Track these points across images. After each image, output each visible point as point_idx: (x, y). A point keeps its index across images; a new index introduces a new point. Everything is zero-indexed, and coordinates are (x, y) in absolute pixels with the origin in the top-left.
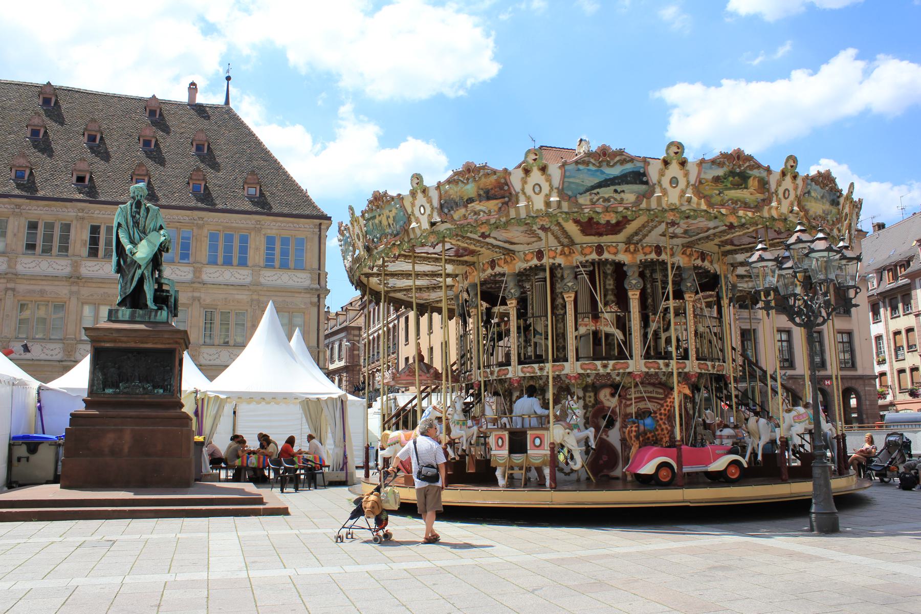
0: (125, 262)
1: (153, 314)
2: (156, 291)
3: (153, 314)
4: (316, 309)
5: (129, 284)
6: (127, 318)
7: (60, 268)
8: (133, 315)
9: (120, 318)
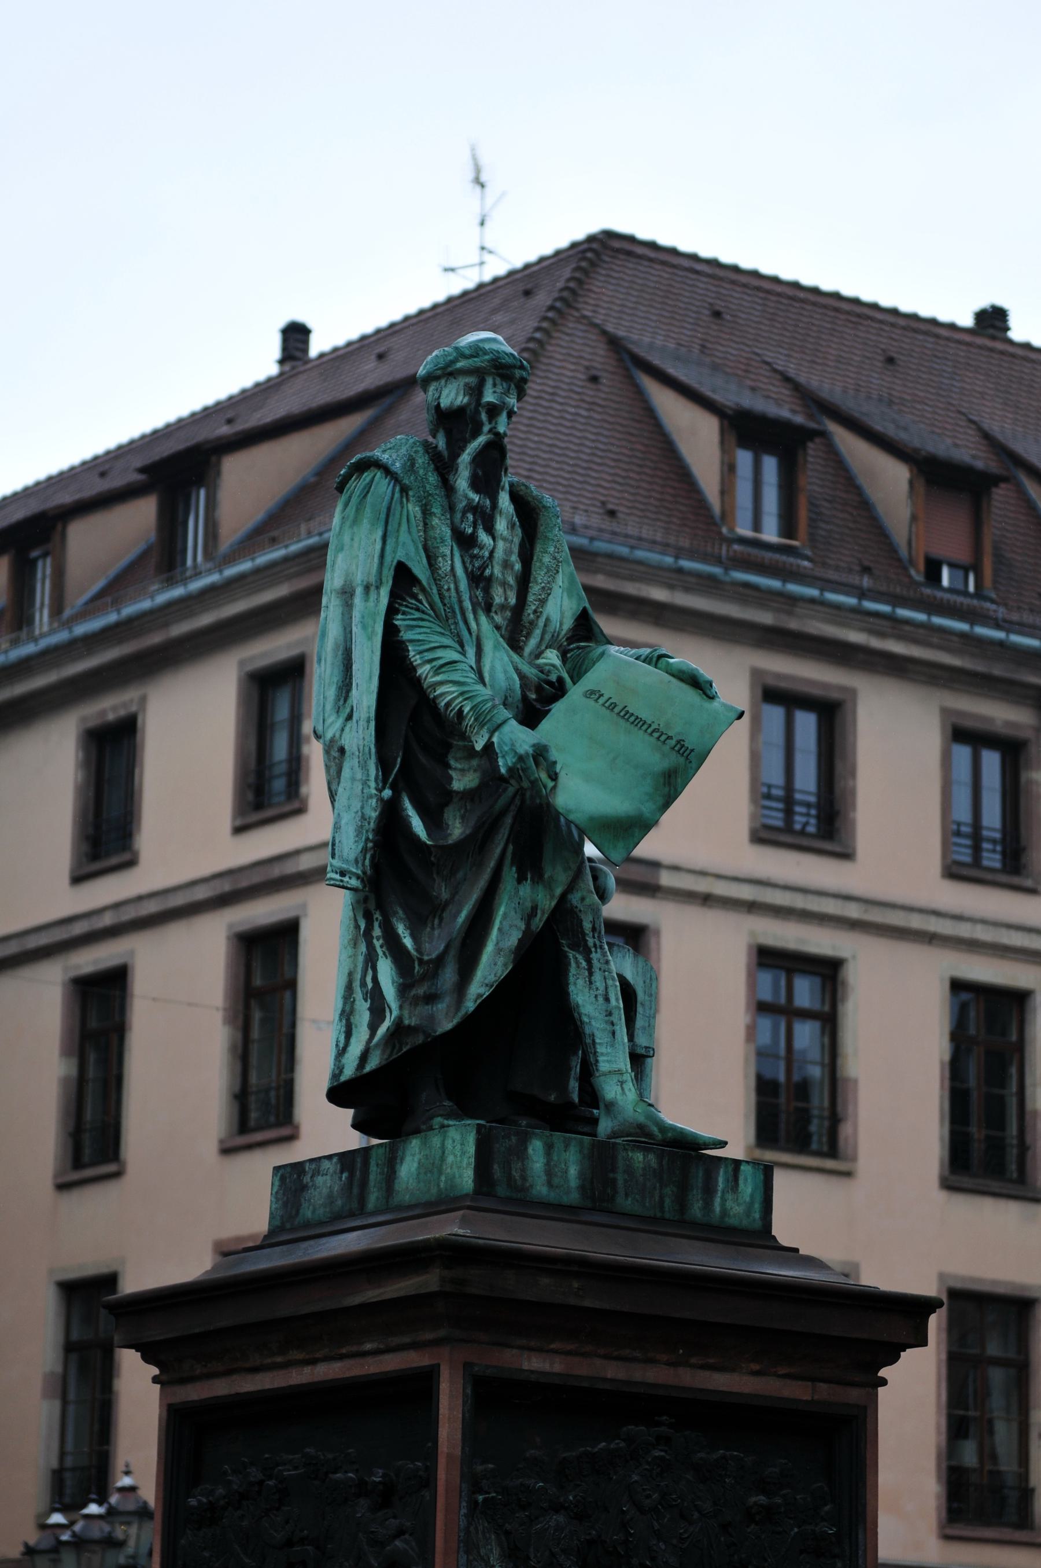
0: (433, 819)
5: (449, 975)
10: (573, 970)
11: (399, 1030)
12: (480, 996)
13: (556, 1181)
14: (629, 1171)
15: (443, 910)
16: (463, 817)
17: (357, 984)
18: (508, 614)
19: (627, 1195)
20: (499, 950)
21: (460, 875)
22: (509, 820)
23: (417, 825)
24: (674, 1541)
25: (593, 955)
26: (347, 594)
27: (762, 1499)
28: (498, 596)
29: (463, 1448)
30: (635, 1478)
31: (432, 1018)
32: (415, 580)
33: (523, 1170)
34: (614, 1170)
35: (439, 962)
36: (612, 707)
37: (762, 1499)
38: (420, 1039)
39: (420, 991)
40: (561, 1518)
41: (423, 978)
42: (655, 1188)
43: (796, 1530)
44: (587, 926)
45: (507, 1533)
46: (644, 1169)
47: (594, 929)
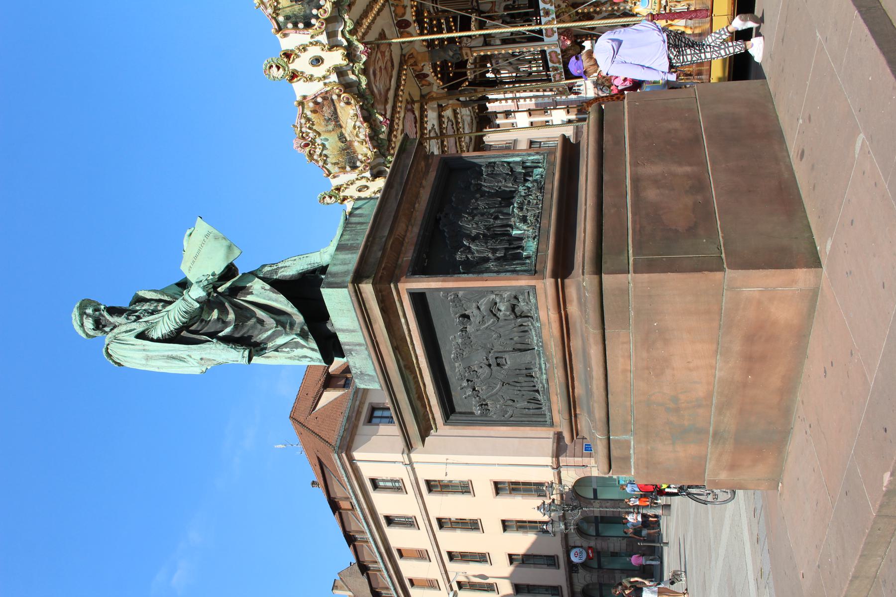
10: (284, 273)
11: (303, 335)
17: (289, 355)
20: (276, 301)
26: (148, 358)
28: (160, 308)
36: (194, 262)
38: (306, 328)
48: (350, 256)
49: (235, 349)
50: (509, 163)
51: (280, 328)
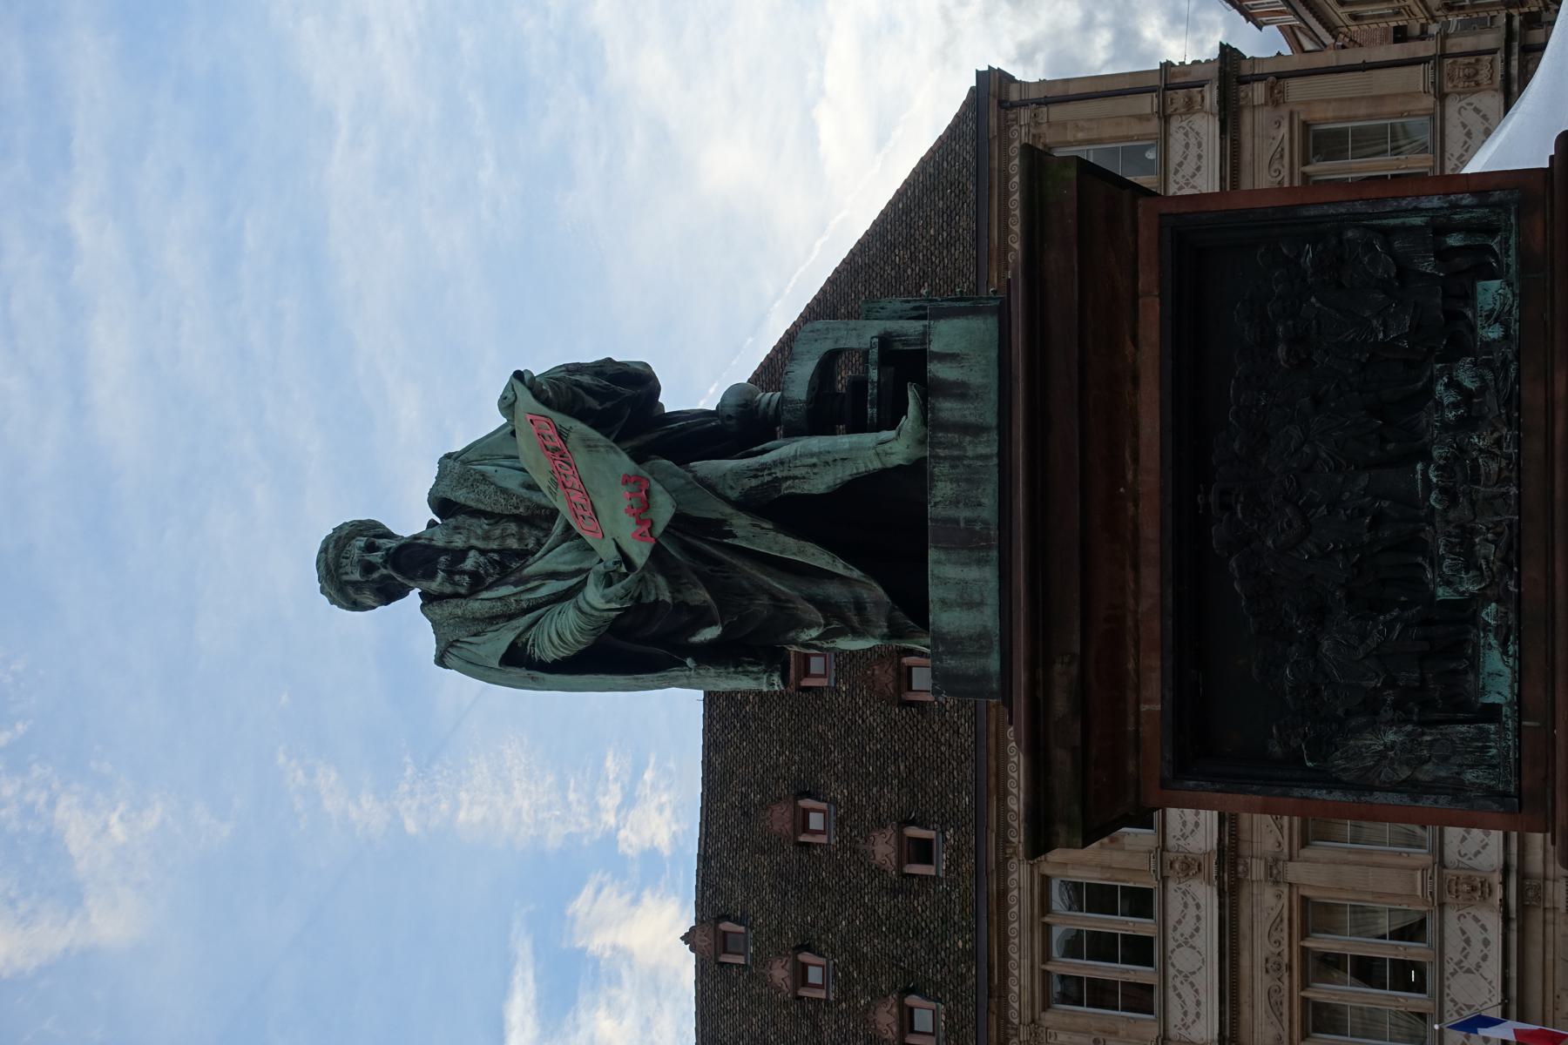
0: (701, 618)
1: (949, 409)
2: (859, 425)
3: (949, 409)
4: (1293, 85)
6: (984, 577)
7: (1192, 911)
8: (965, 541)
9: (987, 618)
12: (845, 567)
13: (977, 597)
14: (955, 502)
15: (779, 600)
16: (695, 586)
18: (526, 530)
19: (980, 505)
20: (801, 552)
21: (745, 583)
22: (688, 539)
23: (711, 633)
24: (1340, 479)
25: (779, 475)
27: (1281, 351)
28: (513, 544)
29: (1254, 793)
30: (1270, 543)
31: (877, 604)
32: (513, 645)
33: (970, 638)
34: (957, 521)
35: (824, 605)
37: (1281, 351)
38: (899, 614)
39: (855, 620)
40: (1326, 644)
41: (843, 619)
42: (969, 466)
43: (1313, 300)
44: (754, 482)
45: (1347, 712)
46: (951, 481)
47: (755, 476)
48: (972, 573)
49: (746, 673)
50: (1387, 233)
51: (835, 625)
